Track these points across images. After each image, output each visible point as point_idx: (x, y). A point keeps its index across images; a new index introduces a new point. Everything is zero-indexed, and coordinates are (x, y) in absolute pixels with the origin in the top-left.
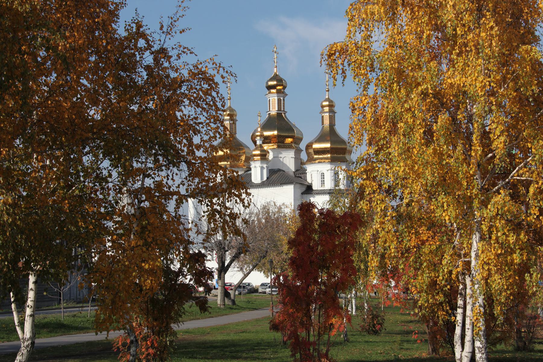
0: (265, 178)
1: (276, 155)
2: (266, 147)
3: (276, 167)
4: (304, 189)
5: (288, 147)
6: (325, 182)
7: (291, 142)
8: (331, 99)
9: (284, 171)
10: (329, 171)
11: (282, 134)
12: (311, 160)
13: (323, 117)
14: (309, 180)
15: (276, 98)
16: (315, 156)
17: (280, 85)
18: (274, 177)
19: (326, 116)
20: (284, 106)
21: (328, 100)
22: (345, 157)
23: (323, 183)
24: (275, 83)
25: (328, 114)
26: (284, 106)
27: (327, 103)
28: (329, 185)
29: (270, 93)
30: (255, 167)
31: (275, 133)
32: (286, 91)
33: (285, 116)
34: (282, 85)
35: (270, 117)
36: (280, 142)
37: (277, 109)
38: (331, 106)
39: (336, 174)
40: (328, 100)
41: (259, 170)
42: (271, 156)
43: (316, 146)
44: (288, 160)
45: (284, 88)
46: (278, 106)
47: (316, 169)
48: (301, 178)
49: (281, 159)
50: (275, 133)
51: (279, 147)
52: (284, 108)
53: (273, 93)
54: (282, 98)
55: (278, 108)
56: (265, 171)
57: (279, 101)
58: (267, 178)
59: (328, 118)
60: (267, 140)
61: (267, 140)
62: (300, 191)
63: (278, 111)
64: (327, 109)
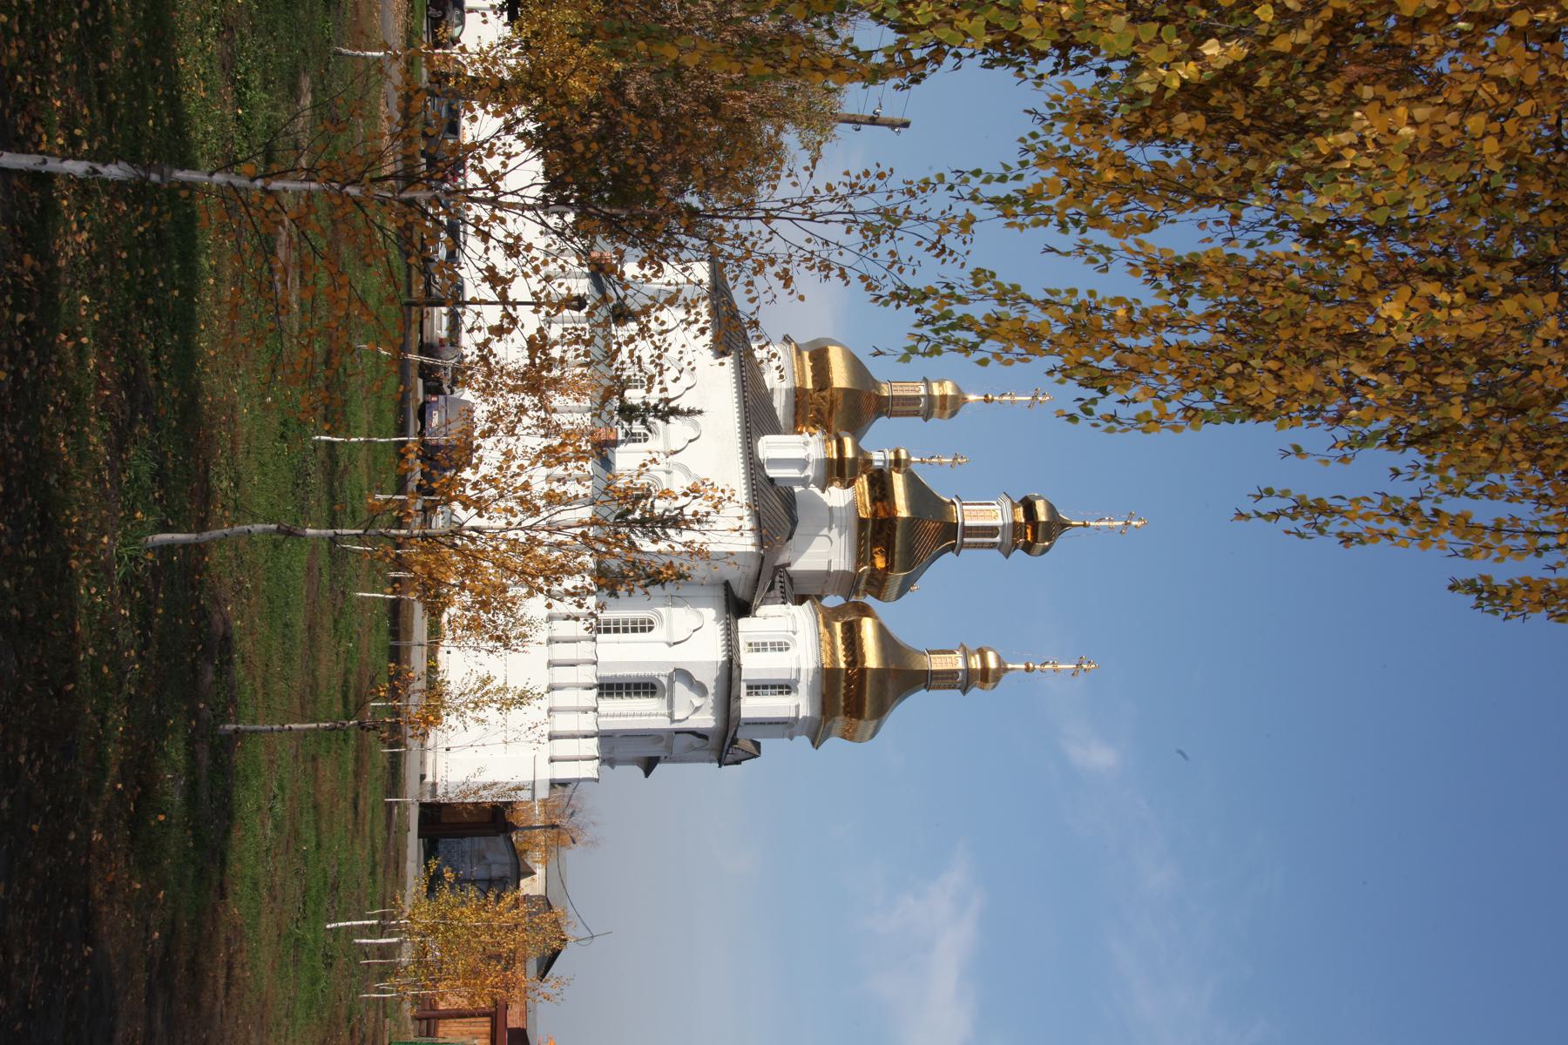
0: (772, 473)
1: (836, 514)
2: (863, 483)
3: (800, 513)
4: (740, 591)
5: (861, 556)
6: (761, 654)
7: (873, 564)
8: (1005, 677)
9: (790, 538)
11: (898, 534)
12: (829, 616)
13: (952, 652)
14: (763, 610)
15: (999, 522)
16: (838, 626)
17: (1035, 533)
18: (776, 502)
19: (955, 662)
21: (1002, 670)
22: (836, 714)
23: (758, 647)
24: (1042, 516)
25: (960, 665)
27: (992, 664)
28: (753, 665)
29: (1014, 506)
30: (806, 444)
31: (903, 512)
32: (1019, 553)
33: (945, 551)
34: (1035, 539)
35: (941, 507)
36: (876, 531)
37: (968, 523)
39: (785, 688)
40: (1002, 670)
41: (799, 454)
42: (837, 497)
43: (868, 628)
44: (825, 552)
45: (1028, 548)
47: (799, 628)
48: (771, 588)
50: (903, 512)
51: (862, 523)
52: (970, 546)
55: (971, 528)
56: (793, 473)
57: (992, 531)
58: (772, 480)
59: (949, 667)
60: (880, 485)
61: (880, 485)
62: (732, 573)
63: (964, 527)
64: (975, 663)
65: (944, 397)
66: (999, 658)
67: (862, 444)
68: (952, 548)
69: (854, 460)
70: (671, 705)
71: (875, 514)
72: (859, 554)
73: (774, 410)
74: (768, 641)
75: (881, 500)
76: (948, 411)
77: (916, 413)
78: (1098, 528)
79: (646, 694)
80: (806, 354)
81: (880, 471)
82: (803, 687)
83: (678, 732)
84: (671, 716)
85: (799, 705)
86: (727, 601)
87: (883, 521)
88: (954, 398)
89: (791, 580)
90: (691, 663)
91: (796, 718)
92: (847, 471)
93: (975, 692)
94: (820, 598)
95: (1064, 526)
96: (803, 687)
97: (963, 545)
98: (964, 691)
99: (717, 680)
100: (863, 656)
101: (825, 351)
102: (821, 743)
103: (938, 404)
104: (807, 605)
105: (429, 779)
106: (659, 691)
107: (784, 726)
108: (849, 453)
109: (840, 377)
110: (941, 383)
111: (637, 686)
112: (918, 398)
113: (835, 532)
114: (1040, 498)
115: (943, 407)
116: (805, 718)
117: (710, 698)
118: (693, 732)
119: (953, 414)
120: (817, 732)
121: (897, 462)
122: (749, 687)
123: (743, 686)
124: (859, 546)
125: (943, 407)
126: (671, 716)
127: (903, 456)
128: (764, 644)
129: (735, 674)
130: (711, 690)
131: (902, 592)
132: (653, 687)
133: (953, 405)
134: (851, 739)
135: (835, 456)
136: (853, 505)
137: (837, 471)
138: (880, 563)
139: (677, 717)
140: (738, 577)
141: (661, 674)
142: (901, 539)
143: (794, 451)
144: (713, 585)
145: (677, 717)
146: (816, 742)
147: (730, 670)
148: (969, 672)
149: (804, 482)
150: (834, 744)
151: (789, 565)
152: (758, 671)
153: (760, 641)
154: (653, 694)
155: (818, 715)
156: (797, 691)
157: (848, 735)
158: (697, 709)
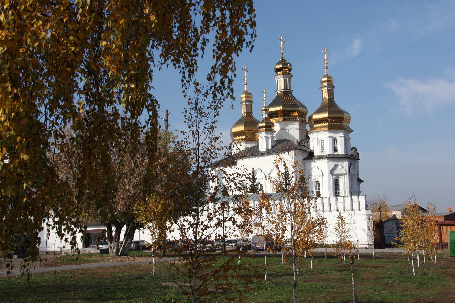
0: (270, 147)
2: (272, 120)
4: (306, 155)
5: (294, 120)
6: (325, 148)
7: (297, 116)
8: (329, 75)
9: (289, 141)
10: (328, 138)
11: (287, 109)
12: (313, 128)
13: (322, 91)
14: (312, 148)
15: (282, 79)
16: (315, 126)
18: (279, 145)
19: (325, 90)
20: (290, 86)
21: (327, 76)
24: (280, 66)
25: (326, 88)
26: (290, 86)
27: (325, 79)
28: (328, 150)
29: (277, 75)
30: (261, 137)
31: (280, 108)
32: (292, 73)
34: (287, 68)
37: (283, 88)
38: (329, 81)
40: (327, 76)
41: (264, 139)
42: (277, 127)
43: (316, 117)
44: (293, 131)
45: (290, 70)
46: (284, 85)
48: (305, 146)
49: (287, 131)
50: (280, 108)
51: (284, 120)
53: (280, 75)
54: (288, 79)
55: (285, 87)
56: (270, 141)
57: (285, 81)
58: (272, 147)
59: (327, 92)
60: (273, 115)
61: (273, 115)
64: (325, 84)
65: (246, 97)
66: (324, 77)
67: (261, 121)
68: (291, 93)
69: (266, 123)
70: (341, 175)
71: (281, 116)
72: (293, 120)
73: (251, 147)
74: (321, 146)
75: (277, 114)
76: (250, 96)
77: (251, 105)
78: (283, 49)
79: (338, 182)
80: (235, 138)
81: (268, 115)
82: (334, 135)
83: (349, 172)
84: (344, 175)
85: (340, 137)
86: (309, 159)
87: (283, 114)
88: (246, 94)
89: (302, 140)
90: (328, 169)
91: (344, 137)
92: (269, 125)
93: (334, 84)
94: (307, 131)
95: (283, 59)
96: (334, 135)
97: (290, 89)
98: (334, 87)
99: (333, 161)
100: (324, 118)
101: (233, 133)
102: (351, 129)
103: (248, 99)
104: (309, 135)
105: (367, 246)
106: (337, 178)
107: (347, 141)
108: (263, 124)
109: (241, 128)
110: (242, 98)
111: (336, 185)
112: (246, 105)
113: (287, 128)
114: (275, 67)
115: (249, 97)
116: (344, 134)
117: (339, 163)
118: (349, 168)
119: (251, 94)
120: (348, 131)
121: (266, 110)
122: (335, 152)
123: (334, 153)
124: (291, 120)
125: (249, 97)
126: (344, 175)
127: (264, 108)
128: (322, 147)
129: (331, 156)
130: (336, 163)
131: (305, 108)
132: (336, 180)
133: (248, 95)
134: (350, 120)
135: (265, 129)
136: (278, 123)
137: (269, 128)
138: (296, 114)
139: (345, 173)
140: (301, 157)
141: (332, 178)
142: (289, 107)
143: (263, 141)
144: (304, 163)
145: (345, 173)
146: (351, 131)
147: (330, 157)
148: (328, 86)
149: (272, 138)
150: (351, 125)
151: (297, 141)
152: (330, 150)
153: (321, 149)
154: (338, 180)
155: (343, 131)
156: (336, 137)
157: (349, 121)
158: (342, 167)
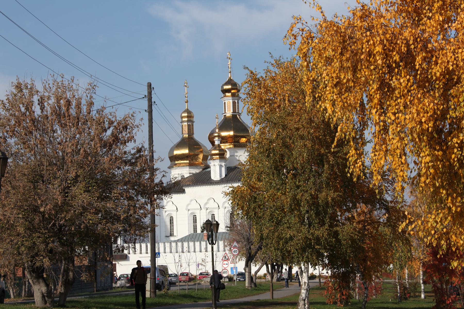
0: (224, 176)
15: (231, 101)
18: (232, 174)
20: (238, 108)
24: (229, 87)
26: (238, 108)
29: (225, 96)
31: (232, 133)
33: (240, 118)
37: (232, 111)
41: (218, 168)
46: (233, 108)
50: (232, 133)
51: (235, 146)
52: (238, 110)
54: (236, 101)
55: (233, 110)
56: (223, 169)
57: (234, 103)
58: (226, 175)
63: (233, 112)
77: (193, 125)
97: (238, 113)
103: (190, 119)
112: (188, 125)
